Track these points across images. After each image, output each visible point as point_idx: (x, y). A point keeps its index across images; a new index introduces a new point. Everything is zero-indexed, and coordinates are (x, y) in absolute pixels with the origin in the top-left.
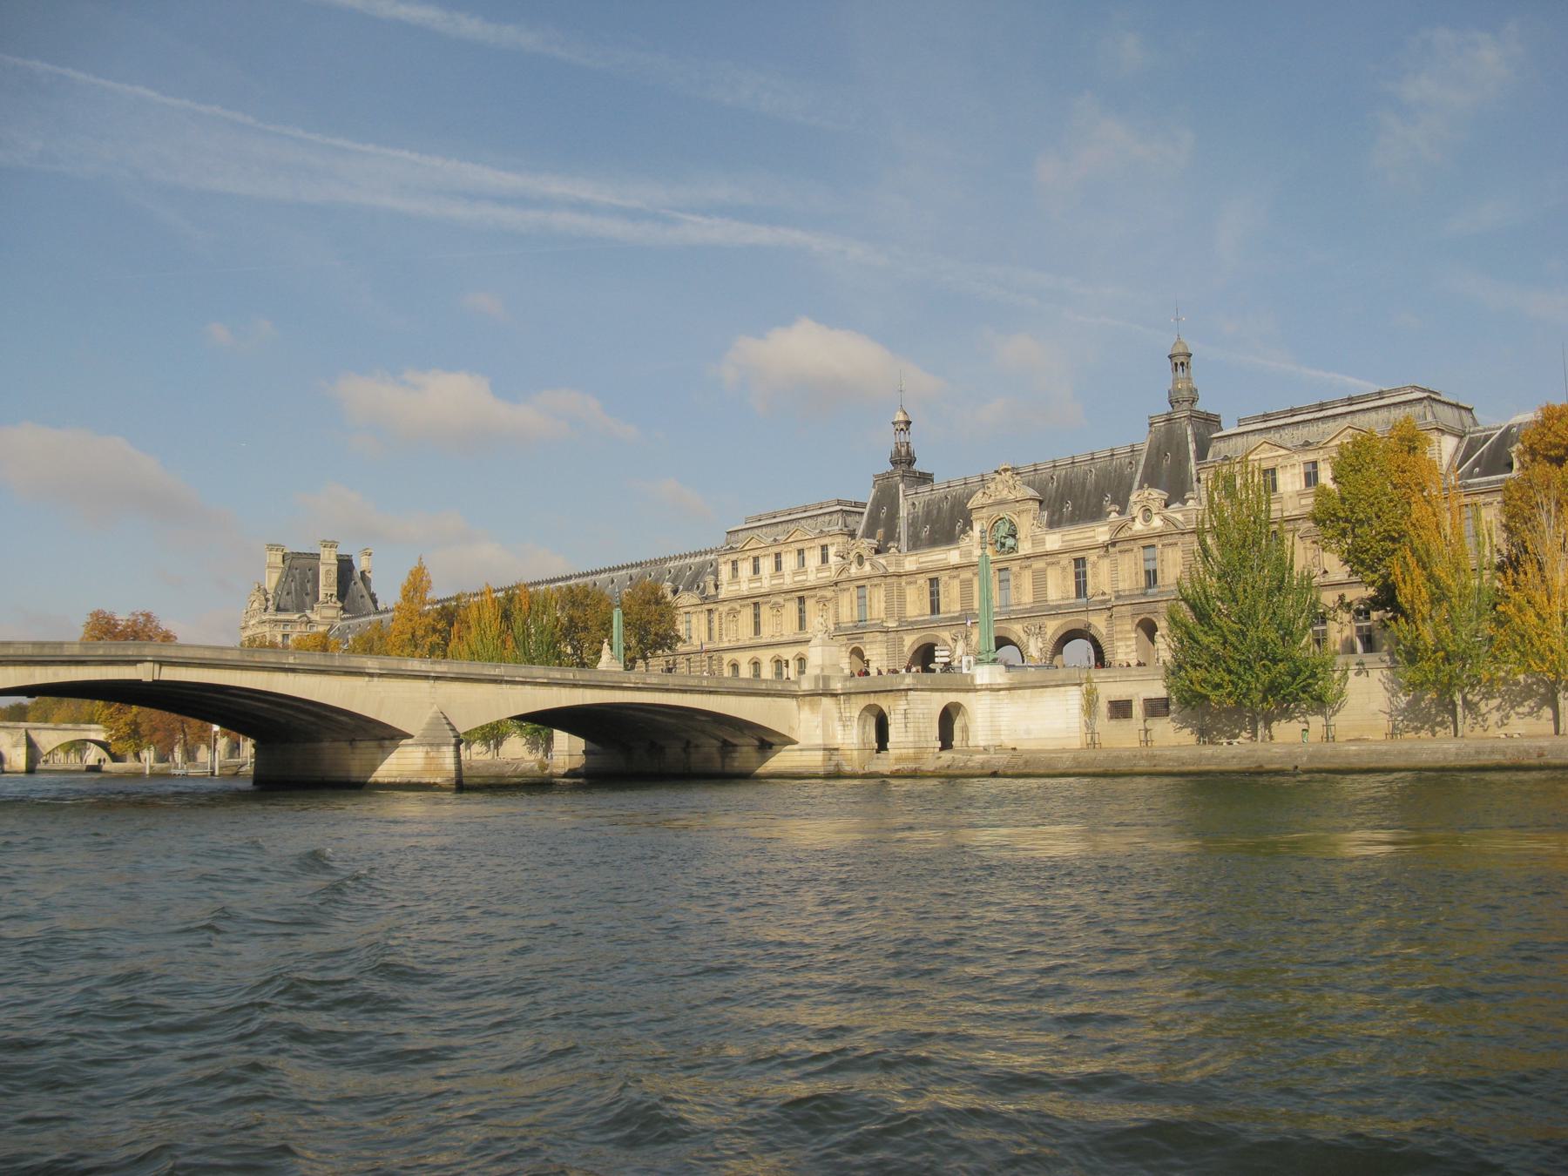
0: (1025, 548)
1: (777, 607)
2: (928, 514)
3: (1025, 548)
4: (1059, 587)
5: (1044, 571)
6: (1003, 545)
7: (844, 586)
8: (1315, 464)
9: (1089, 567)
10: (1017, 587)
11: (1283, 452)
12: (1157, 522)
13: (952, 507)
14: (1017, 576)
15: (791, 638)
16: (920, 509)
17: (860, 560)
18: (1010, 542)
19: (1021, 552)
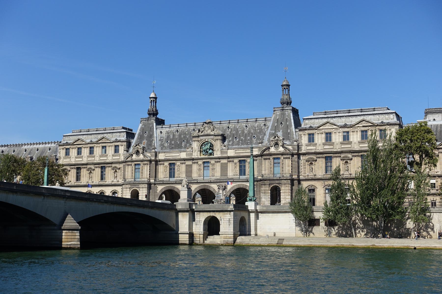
1: (90, 171)
2: (168, 137)
3: (217, 154)
4: (232, 171)
5: (226, 164)
6: (207, 152)
7: (130, 163)
8: (348, 132)
9: (247, 164)
10: (213, 169)
11: (335, 127)
12: (281, 149)
13: (180, 135)
14: (213, 165)
15: (97, 183)
16: (164, 135)
17: (137, 153)
18: (211, 151)
19: (215, 156)
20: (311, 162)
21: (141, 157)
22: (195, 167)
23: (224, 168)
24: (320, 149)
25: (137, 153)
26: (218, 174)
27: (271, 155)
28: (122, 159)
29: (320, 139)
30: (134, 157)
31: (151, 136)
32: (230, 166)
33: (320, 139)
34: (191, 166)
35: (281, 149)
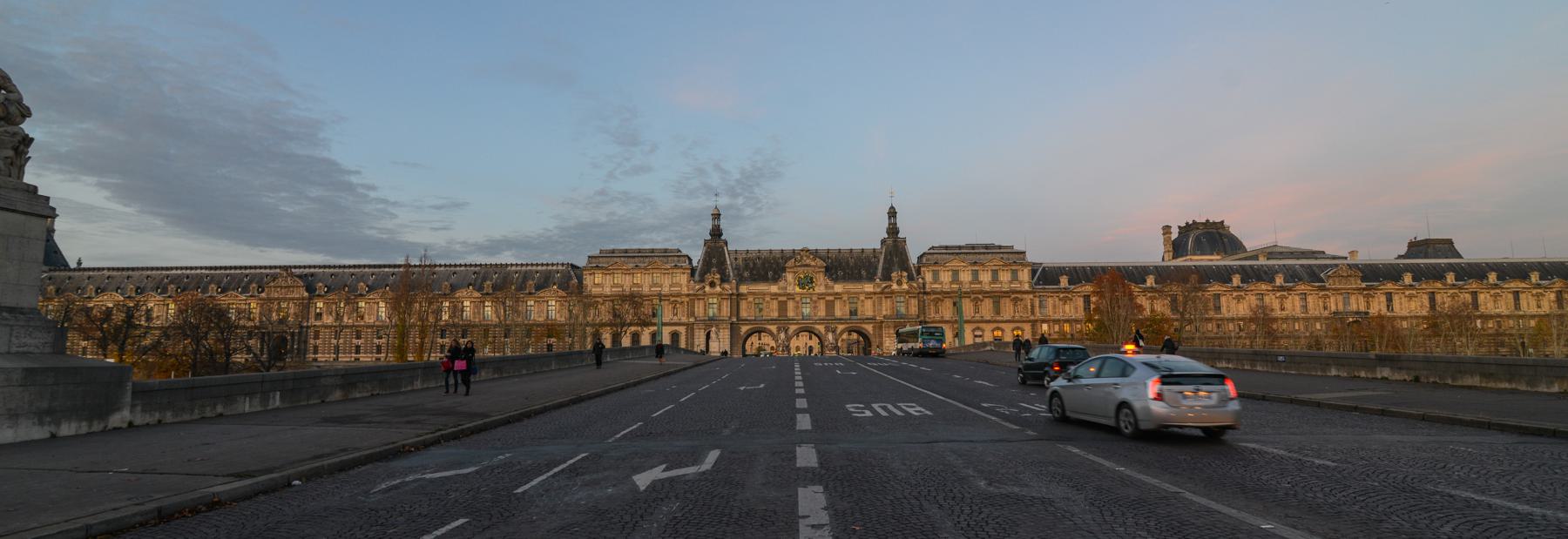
0: (820, 289)
12: (905, 286)
16: (740, 262)
20: (936, 301)
21: (718, 289)
22: (791, 305)
23: (830, 306)
24: (946, 288)
25: (712, 285)
26: (822, 313)
27: (893, 292)
28: (685, 291)
29: (945, 277)
30: (707, 289)
31: (722, 263)
32: (838, 304)
33: (945, 277)
34: (785, 303)
35: (905, 286)
